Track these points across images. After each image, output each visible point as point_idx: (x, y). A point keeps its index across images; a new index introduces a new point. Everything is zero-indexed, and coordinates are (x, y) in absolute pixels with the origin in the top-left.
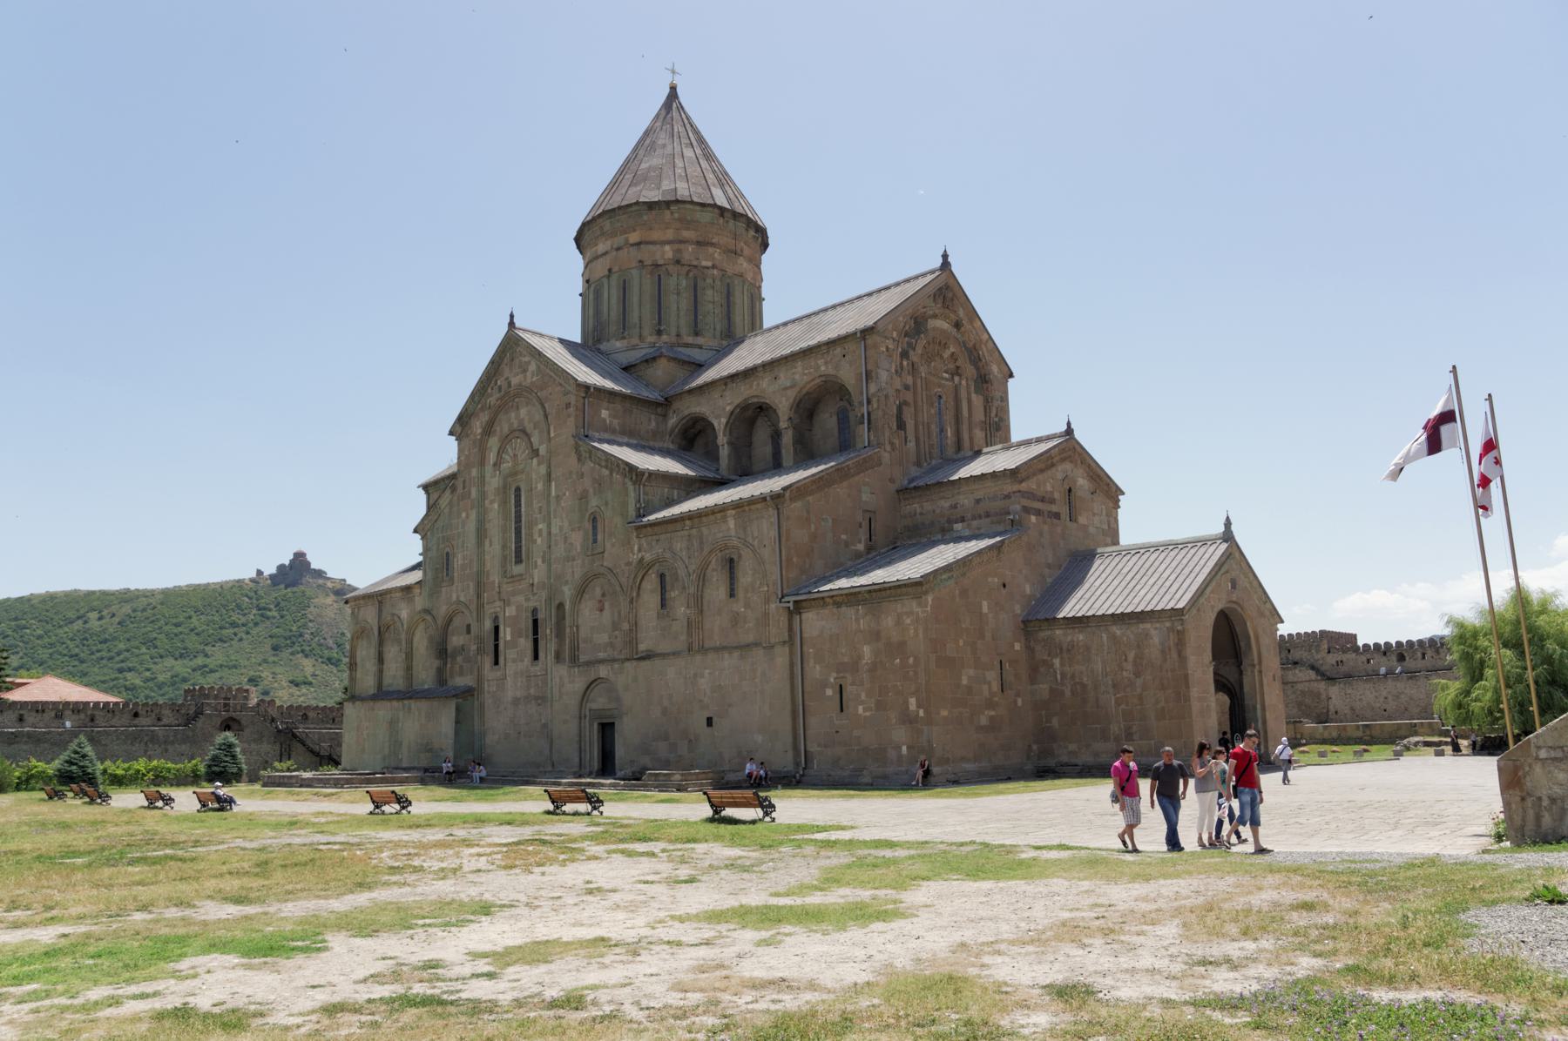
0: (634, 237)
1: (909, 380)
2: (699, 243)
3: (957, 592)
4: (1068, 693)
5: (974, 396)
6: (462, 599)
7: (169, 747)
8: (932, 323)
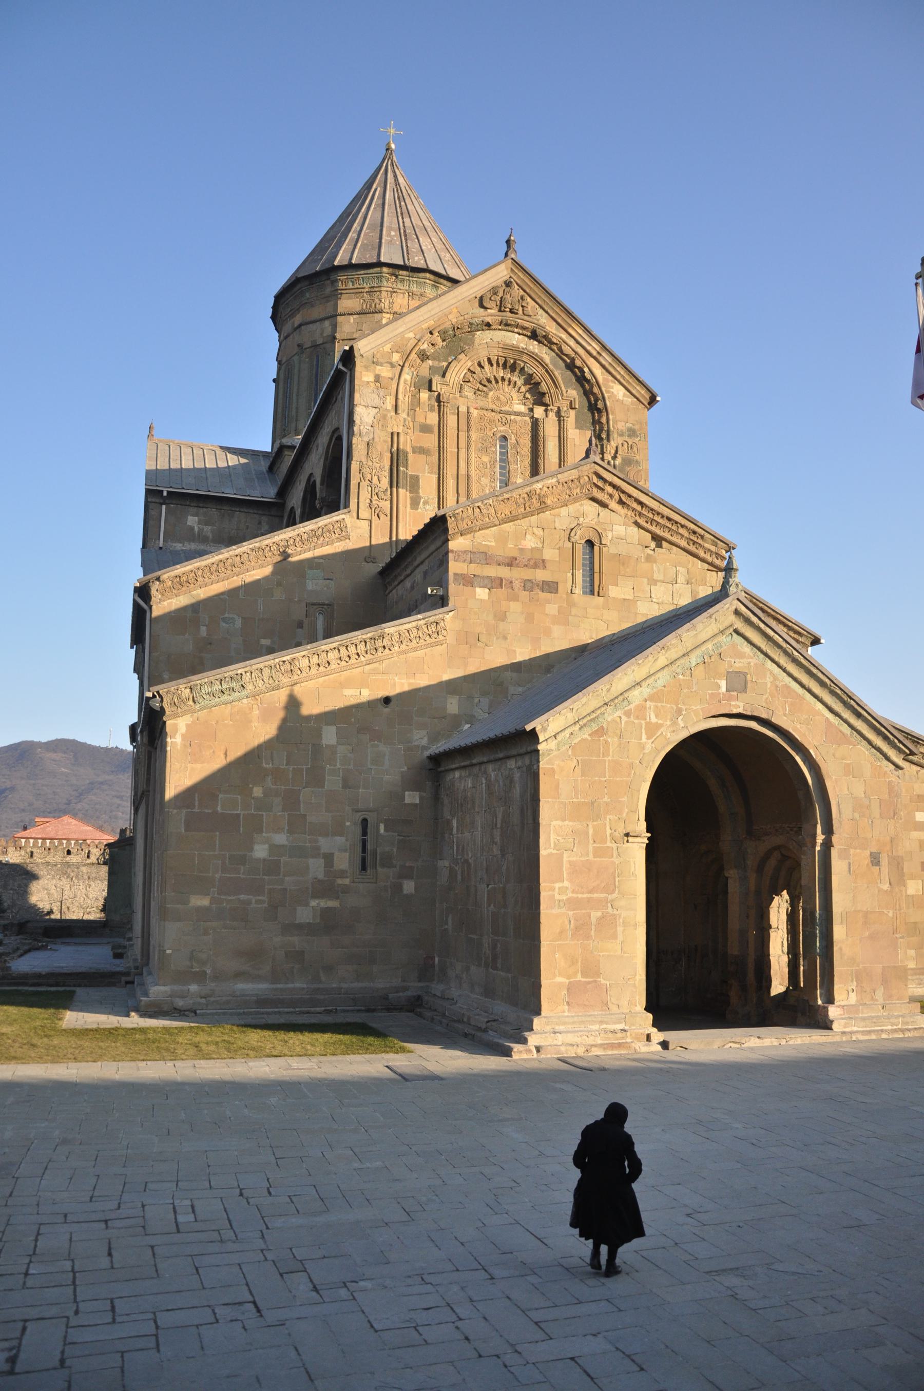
0: (297, 320)
3: (257, 712)
4: (459, 877)
7: (92, 883)
8: (482, 337)
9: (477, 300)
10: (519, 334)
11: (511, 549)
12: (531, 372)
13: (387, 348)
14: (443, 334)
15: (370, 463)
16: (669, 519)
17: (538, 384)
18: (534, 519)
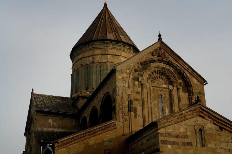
0: (80, 56)
1: (139, 90)
5: (182, 94)
8: (153, 65)
9: (151, 53)
10: (164, 63)
11: (177, 132)
12: (168, 75)
13: (125, 68)
14: (141, 64)
15: (122, 104)
16: (224, 122)
17: (170, 78)
18: (183, 122)
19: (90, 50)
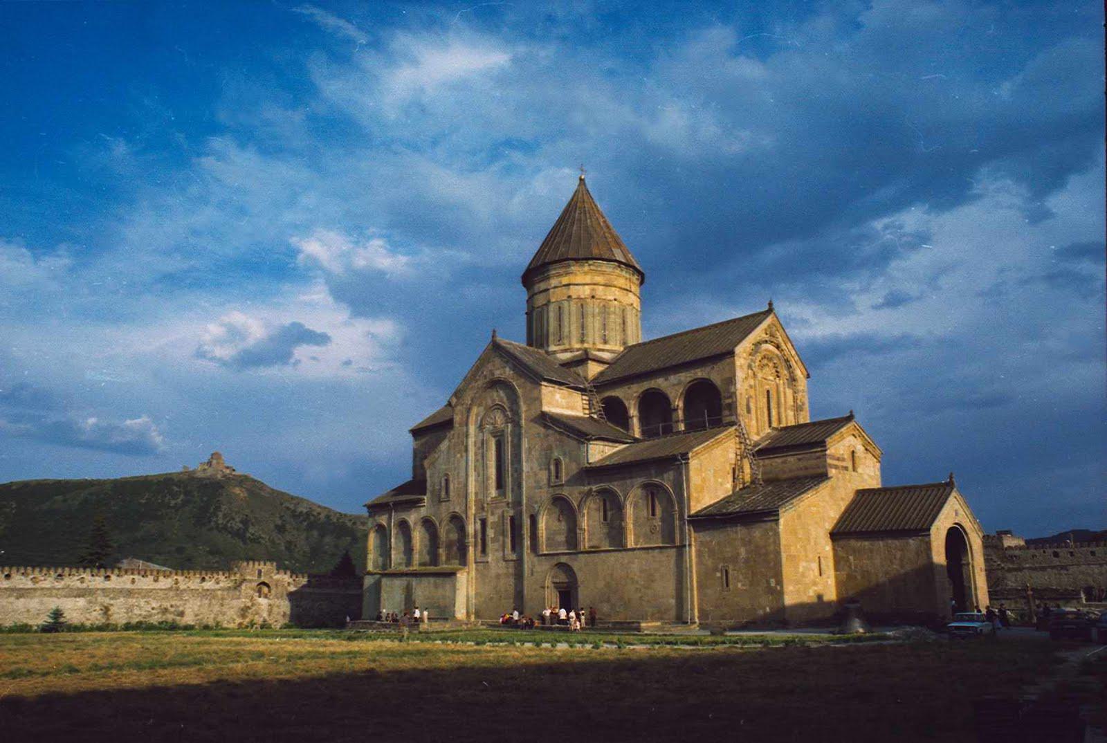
1: (752, 382)
2: (606, 285)
4: (859, 577)
6: (457, 510)
8: (765, 346)
17: (777, 367)
19: (586, 273)
